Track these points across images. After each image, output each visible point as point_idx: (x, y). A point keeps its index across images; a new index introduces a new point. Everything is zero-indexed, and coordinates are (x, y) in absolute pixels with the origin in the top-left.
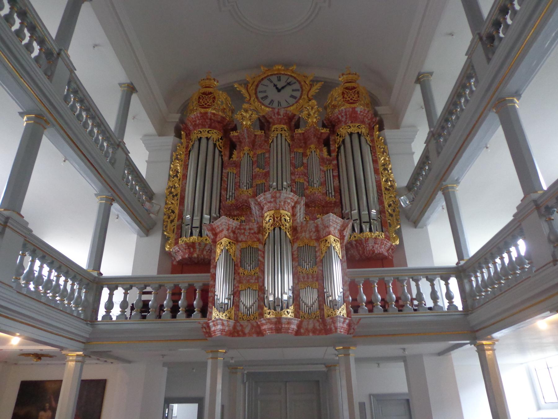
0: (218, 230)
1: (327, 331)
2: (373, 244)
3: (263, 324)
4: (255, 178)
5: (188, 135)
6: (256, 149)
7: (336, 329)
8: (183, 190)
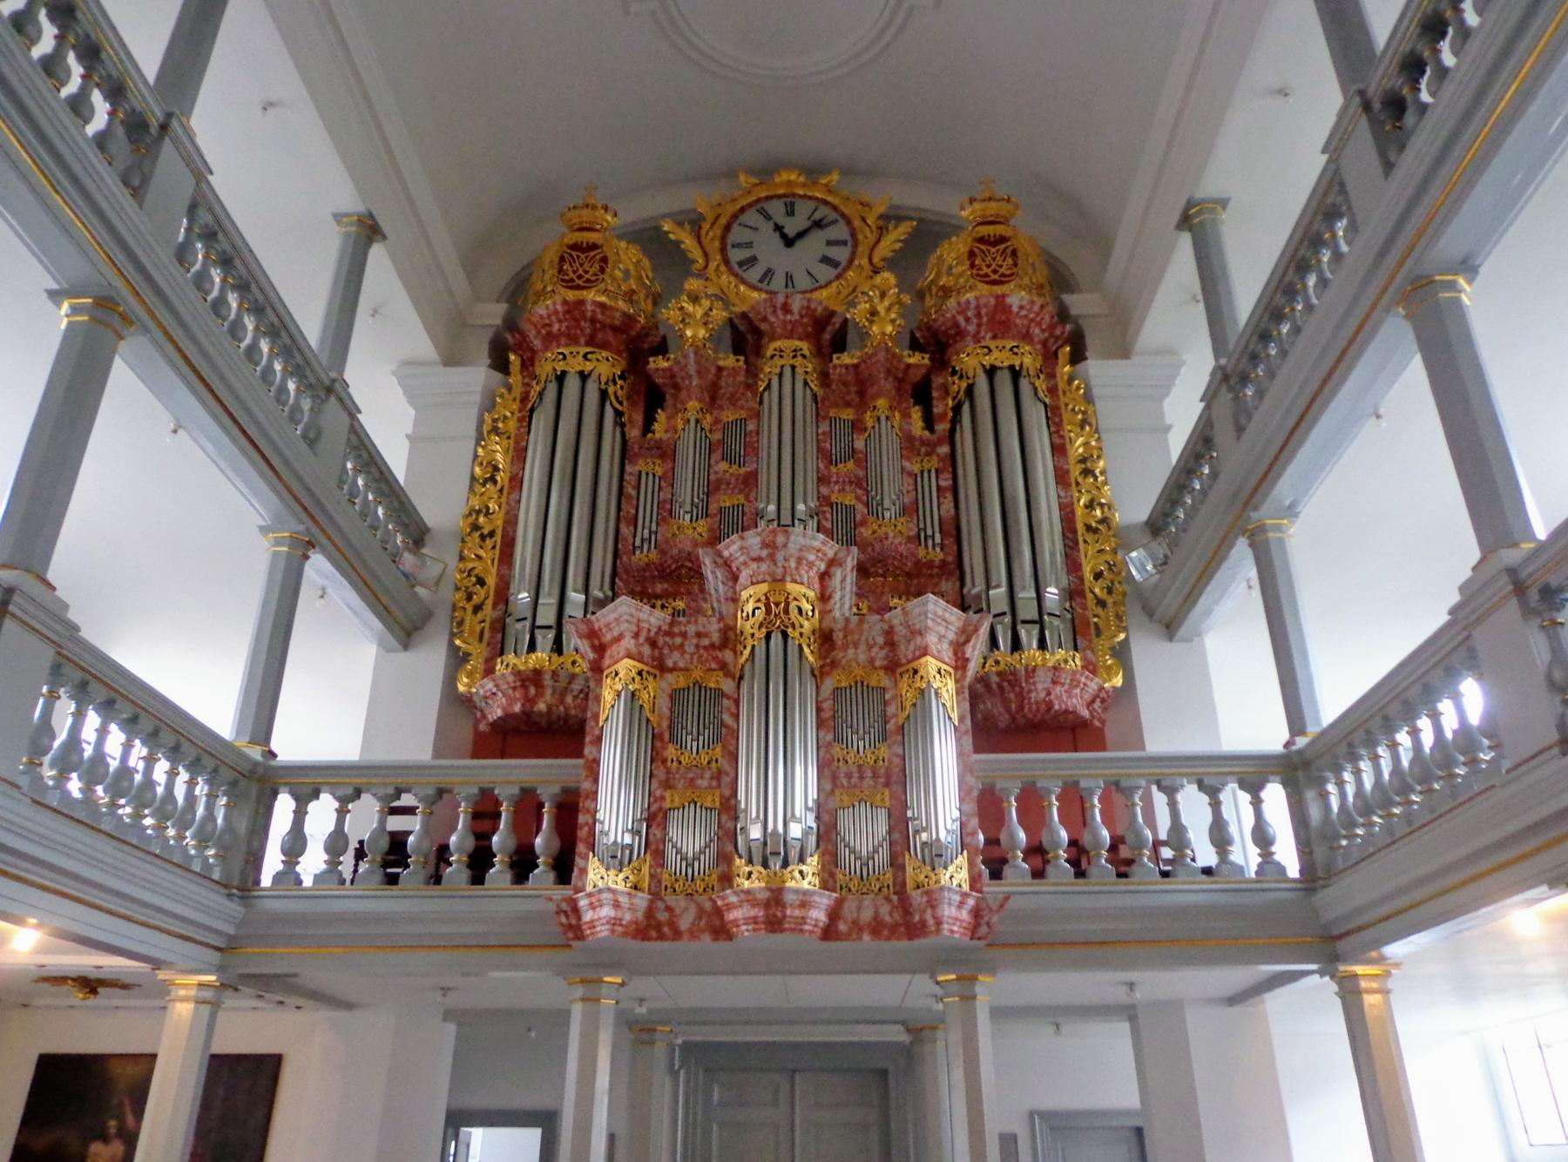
0: (608, 637)
1: (914, 930)
2: (1048, 685)
3: (730, 907)
4: (717, 489)
5: (528, 364)
6: (721, 408)
7: (939, 923)
8: (511, 521)
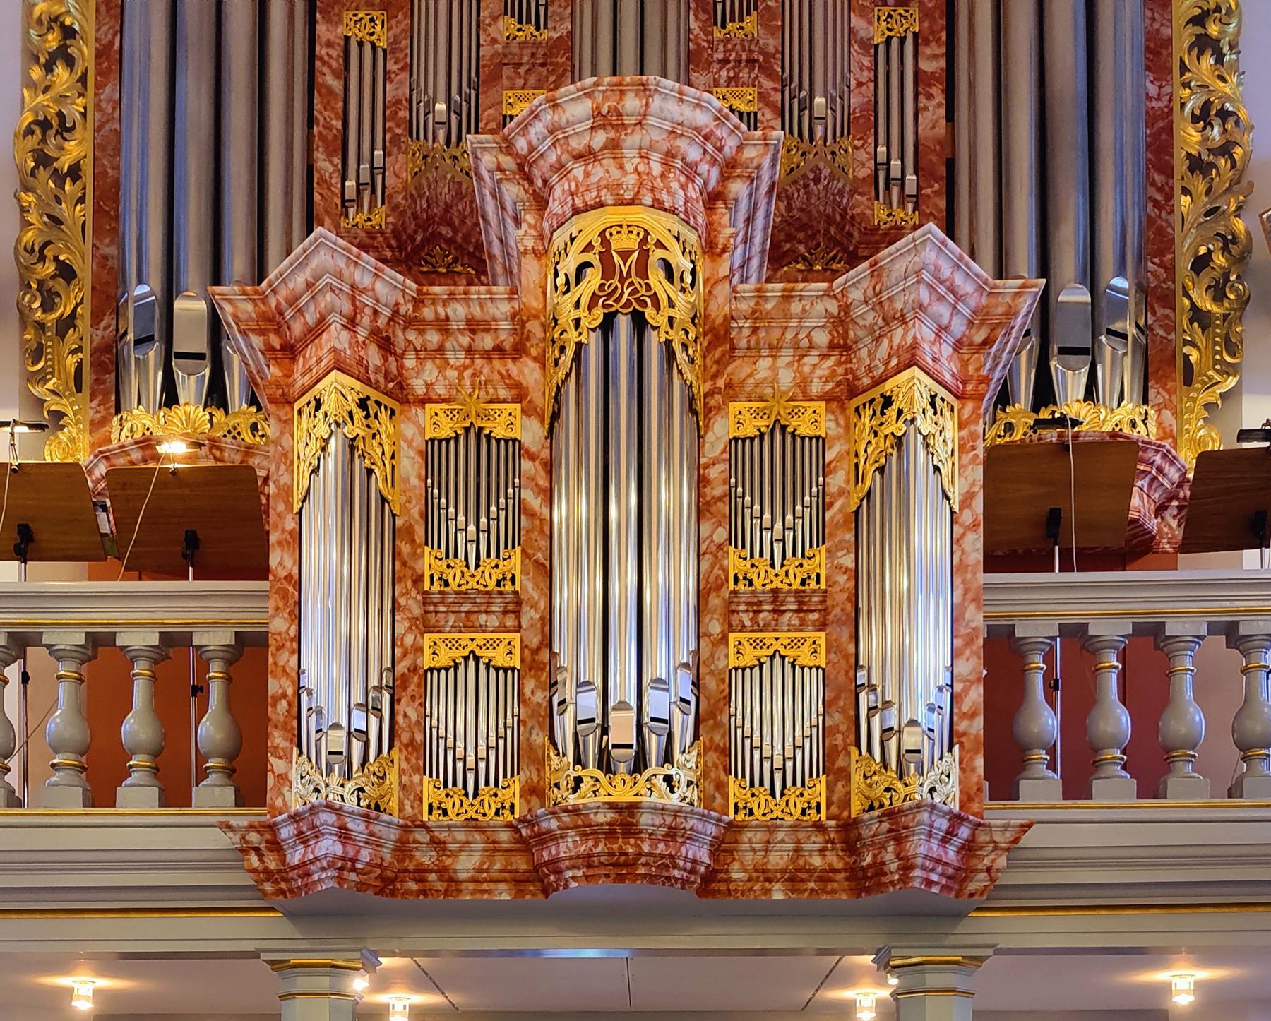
4: (495, 77)
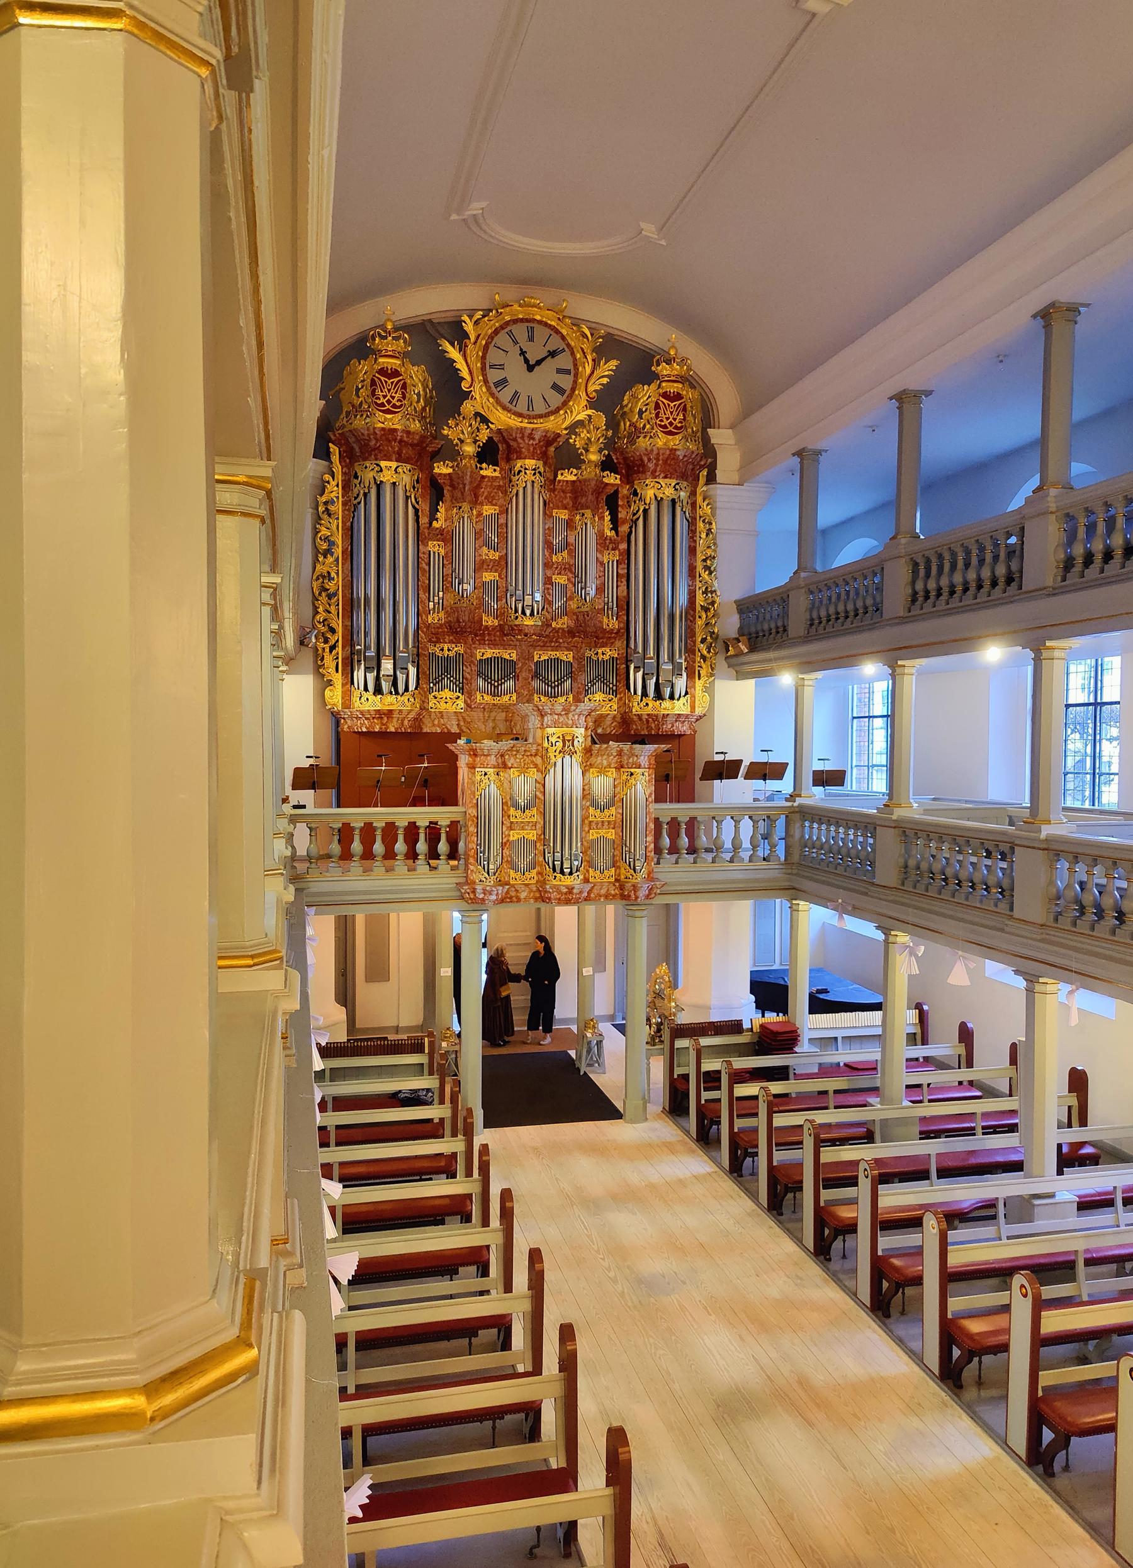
6: (482, 504)
